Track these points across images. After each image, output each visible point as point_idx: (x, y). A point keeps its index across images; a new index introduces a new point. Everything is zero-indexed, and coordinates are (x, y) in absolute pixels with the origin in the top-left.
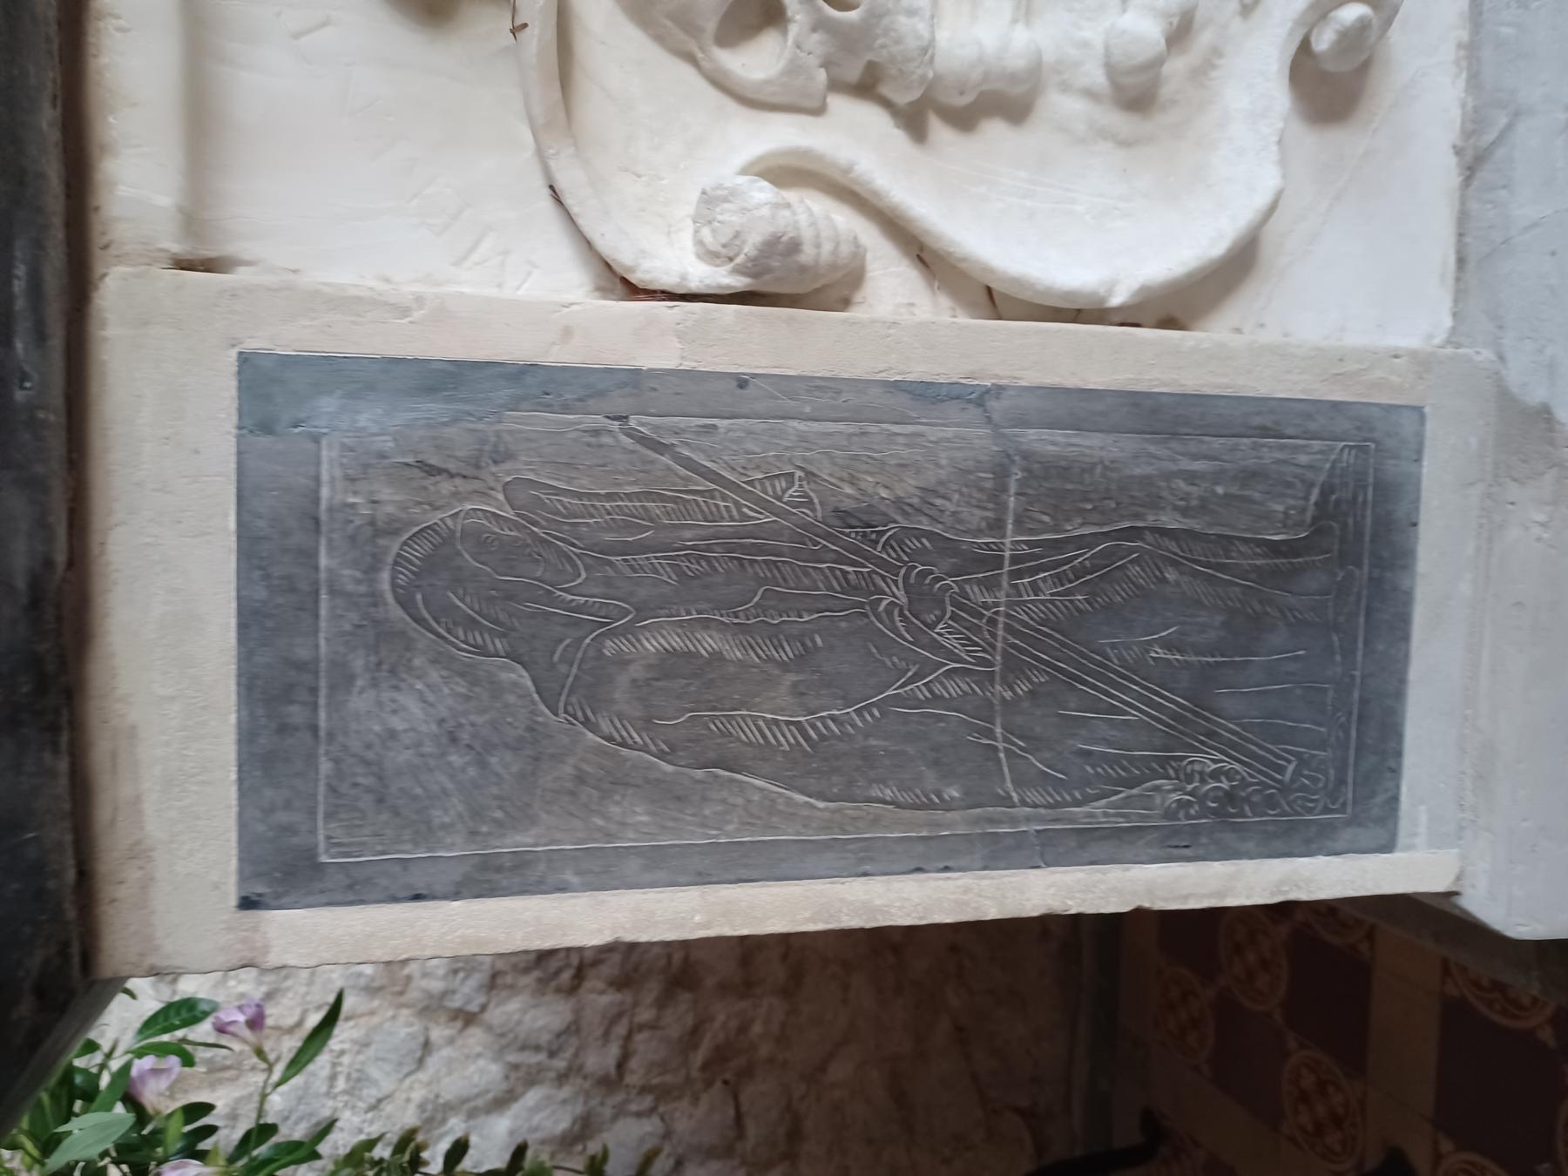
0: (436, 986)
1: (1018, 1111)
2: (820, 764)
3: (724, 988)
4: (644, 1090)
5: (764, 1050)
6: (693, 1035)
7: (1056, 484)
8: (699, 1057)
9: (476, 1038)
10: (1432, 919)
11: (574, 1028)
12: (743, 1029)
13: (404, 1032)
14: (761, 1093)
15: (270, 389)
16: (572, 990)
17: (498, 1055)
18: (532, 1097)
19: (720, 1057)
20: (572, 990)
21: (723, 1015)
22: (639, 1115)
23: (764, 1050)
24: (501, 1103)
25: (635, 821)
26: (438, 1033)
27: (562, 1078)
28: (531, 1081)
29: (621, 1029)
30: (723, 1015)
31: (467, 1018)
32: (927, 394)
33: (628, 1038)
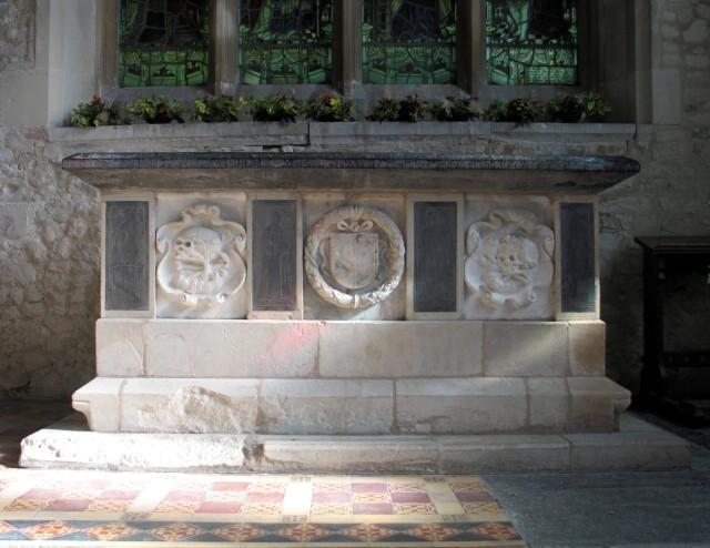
0: (75, 224)
1: (29, 383)
2: (116, 249)
3: (68, 298)
4: (44, 278)
5: (51, 309)
6: (56, 289)
7: (140, 271)
8: (51, 291)
9: (61, 234)
10: (99, 317)
11: (62, 259)
12: (58, 304)
13: (64, 216)
14: (39, 309)
15: (146, 204)
16: (72, 258)
17: (57, 240)
18: (45, 248)
19: (49, 296)
20: (72, 258)
21: (61, 298)
22: (37, 276)
23: (51, 309)
24: (44, 240)
25: (111, 232)
26: (63, 225)
27: (48, 256)
28: (49, 248)
29: (60, 271)
30: (61, 298)
31: (66, 232)
32: (148, 258)
33: (58, 273)
